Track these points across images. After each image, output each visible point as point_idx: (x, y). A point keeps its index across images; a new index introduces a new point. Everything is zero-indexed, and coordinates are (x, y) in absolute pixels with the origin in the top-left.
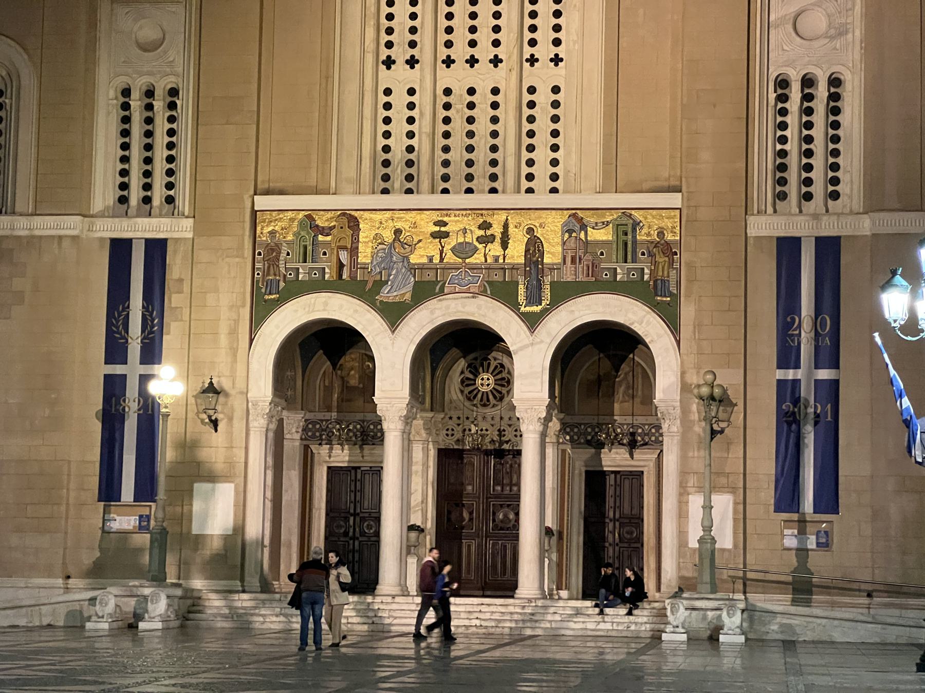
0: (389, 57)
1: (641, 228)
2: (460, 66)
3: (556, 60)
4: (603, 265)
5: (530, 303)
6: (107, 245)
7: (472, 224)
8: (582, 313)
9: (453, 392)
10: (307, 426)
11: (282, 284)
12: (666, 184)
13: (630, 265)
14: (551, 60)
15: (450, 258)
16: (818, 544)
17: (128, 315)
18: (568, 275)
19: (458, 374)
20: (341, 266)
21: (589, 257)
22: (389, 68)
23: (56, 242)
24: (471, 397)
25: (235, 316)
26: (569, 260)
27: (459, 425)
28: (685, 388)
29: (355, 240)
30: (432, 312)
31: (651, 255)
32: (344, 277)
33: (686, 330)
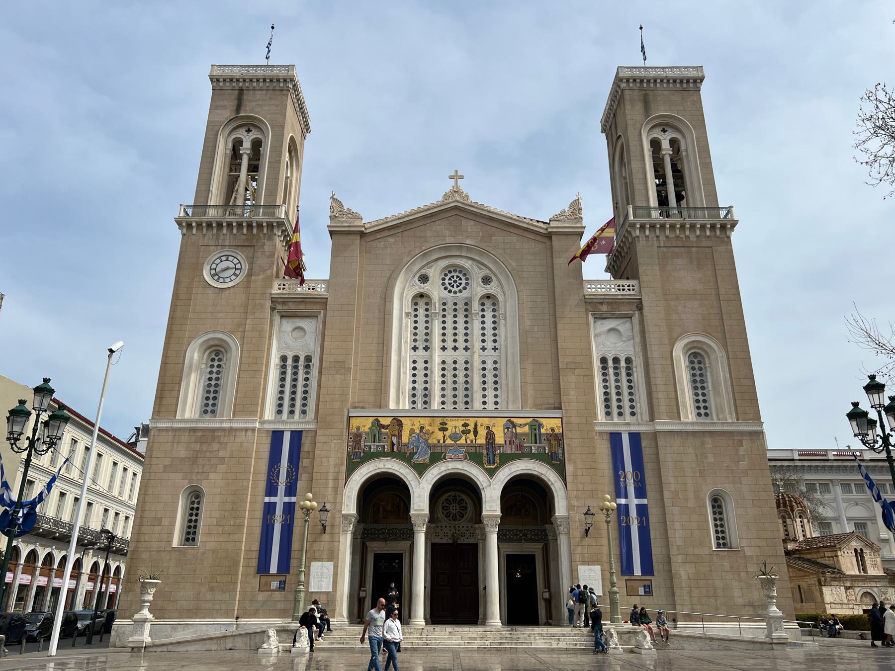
0: (415, 346)
1: (543, 427)
2: (450, 351)
3: (495, 349)
4: (525, 445)
5: (489, 464)
6: (271, 434)
7: (460, 423)
8: (516, 469)
9: (438, 513)
11: (362, 454)
12: (552, 406)
13: (538, 445)
14: (493, 349)
15: (449, 441)
16: (645, 592)
17: (279, 471)
18: (508, 450)
19: (441, 504)
20: (393, 444)
21: (517, 441)
22: (415, 351)
23: (244, 431)
25: (337, 470)
26: (508, 443)
28: (570, 507)
29: (400, 430)
30: (440, 469)
31: (548, 440)
32: (395, 450)
33: (569, 479)
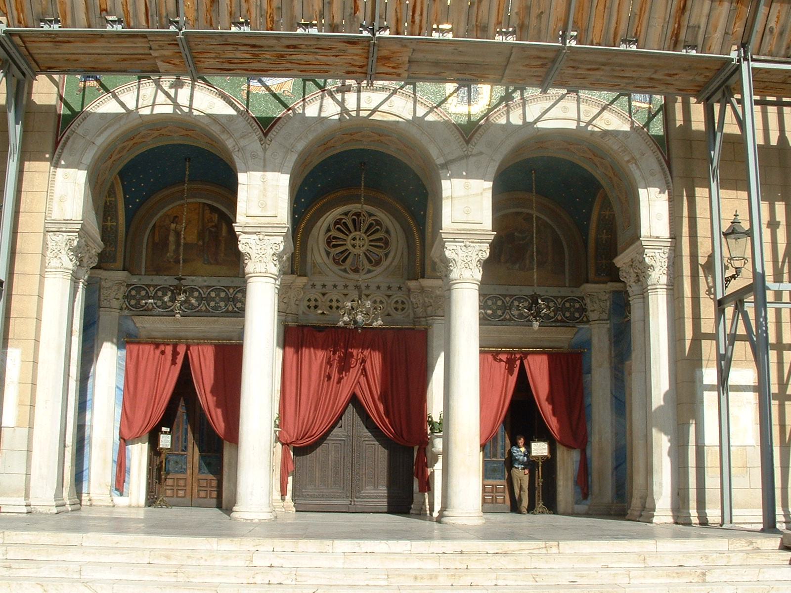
10: (130, 291)
24: (340, 260)
27: (324, 295)
